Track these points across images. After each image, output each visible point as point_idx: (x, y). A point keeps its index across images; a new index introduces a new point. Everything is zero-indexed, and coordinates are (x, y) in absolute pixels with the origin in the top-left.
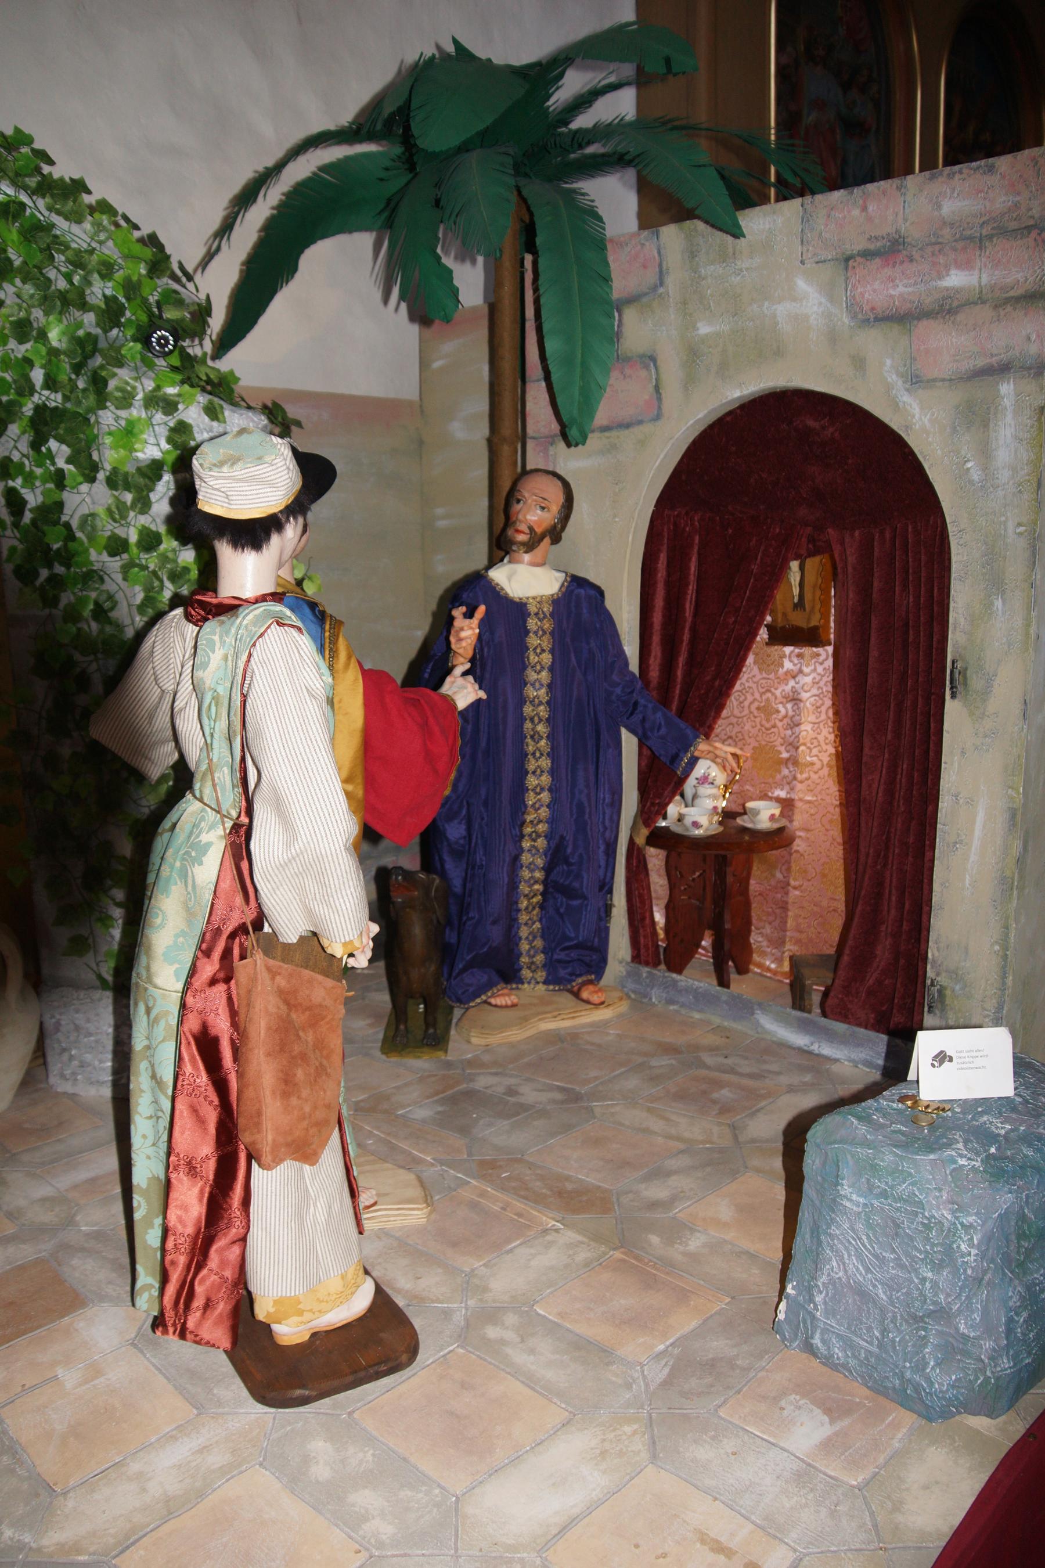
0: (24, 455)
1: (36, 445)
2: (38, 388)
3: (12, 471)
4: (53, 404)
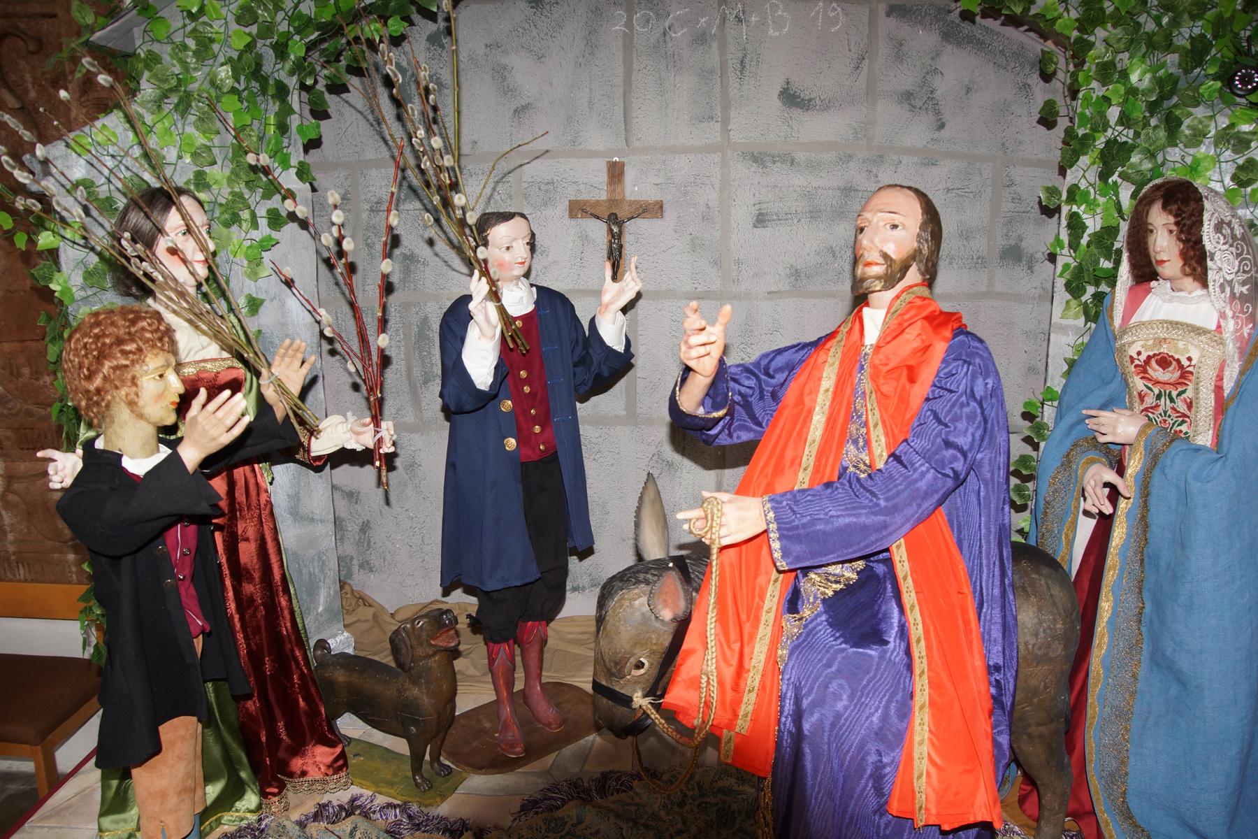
0: (1091, 185)
1: (1104, 176)
2: (1112, 123)
3: (1077, 198)
4: (1124, 139)
